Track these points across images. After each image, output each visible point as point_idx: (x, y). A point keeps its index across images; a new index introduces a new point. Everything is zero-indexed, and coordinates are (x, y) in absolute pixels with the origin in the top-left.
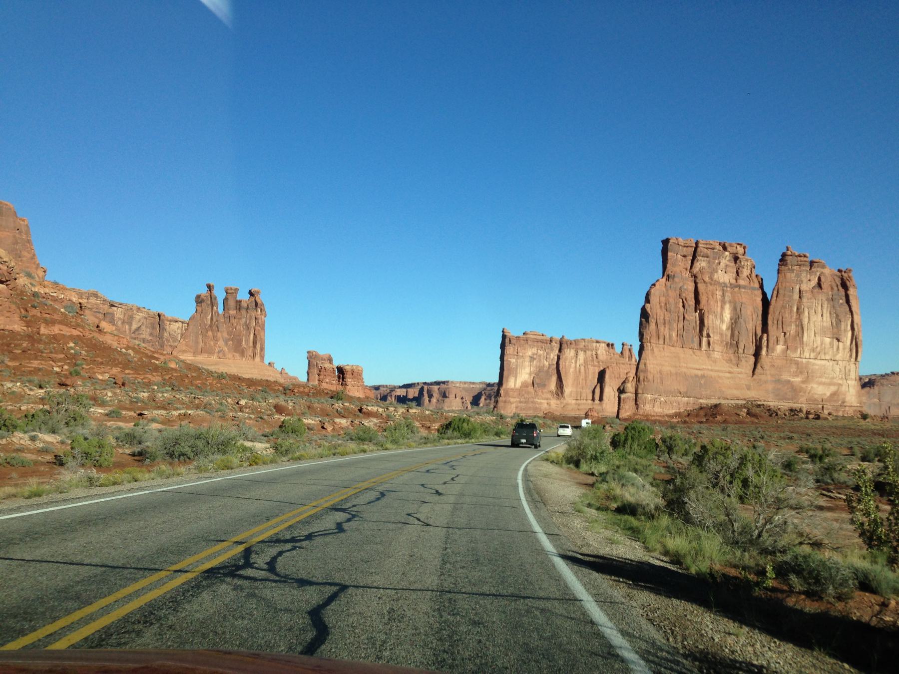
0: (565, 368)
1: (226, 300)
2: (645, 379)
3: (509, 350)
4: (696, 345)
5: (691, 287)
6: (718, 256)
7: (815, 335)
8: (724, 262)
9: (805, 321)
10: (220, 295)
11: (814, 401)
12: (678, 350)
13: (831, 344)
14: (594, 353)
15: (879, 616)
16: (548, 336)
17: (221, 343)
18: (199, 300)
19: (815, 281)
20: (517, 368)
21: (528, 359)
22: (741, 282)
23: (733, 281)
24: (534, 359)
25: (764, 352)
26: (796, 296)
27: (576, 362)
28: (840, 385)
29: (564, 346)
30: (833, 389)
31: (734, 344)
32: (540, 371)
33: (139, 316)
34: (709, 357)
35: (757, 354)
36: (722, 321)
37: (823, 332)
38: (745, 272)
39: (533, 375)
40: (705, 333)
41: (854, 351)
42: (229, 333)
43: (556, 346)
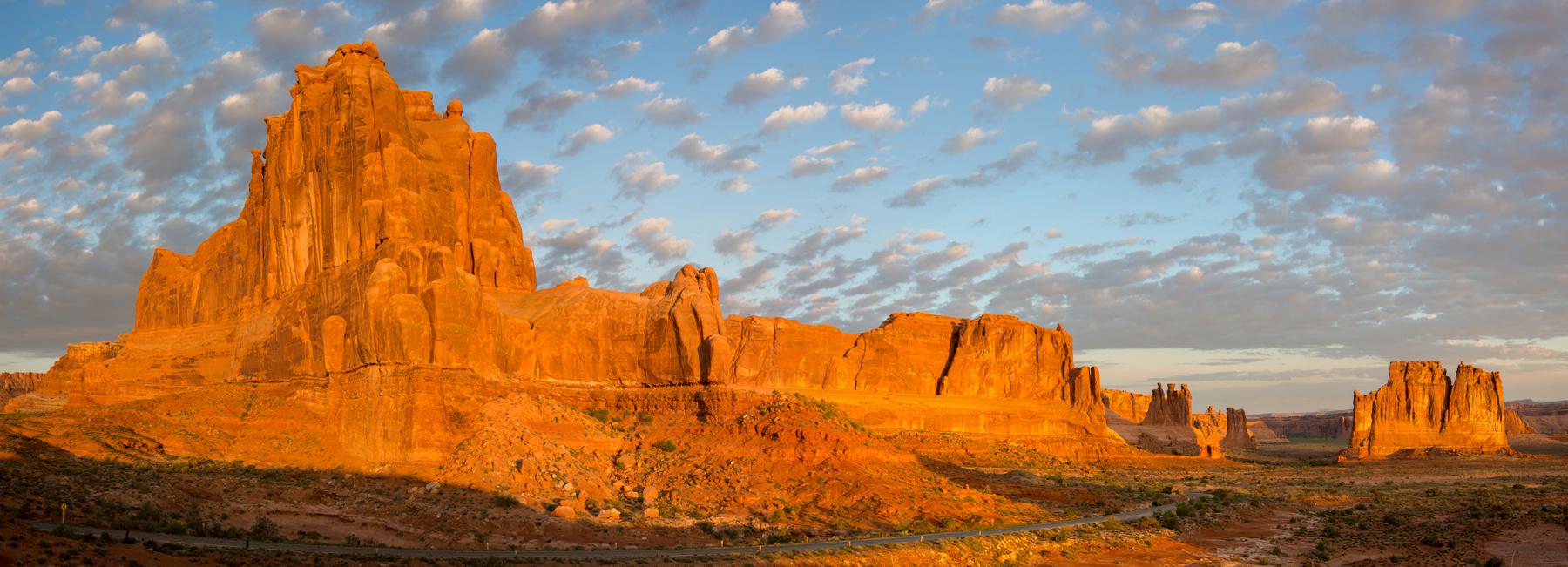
1: (1168, 392)
4: (1406, 418)
5: (1404, 388)
6: (1420, 369)
8: (1424, 372)
10: (1165, 389)
11: (1478, 444)
12: (1395, 422)
13: (1486, 413)
17: (1167, 416)
18: (1154, 392)
19: (1476, 380)
22: (1435, 382)
23: (1430, 382)
25: (1446, 420)
26: (1465, 388)
28: (1492, 434)
30: (1488, 436)
31: (1430, 416)
33: (1120, 397)
34: (1414, 423)
35: (1443, 420)
36: (1423, 403)
37: (1482, 406)
38: (1437, 377)
40: (1411, 412)
42: (1172, 411)
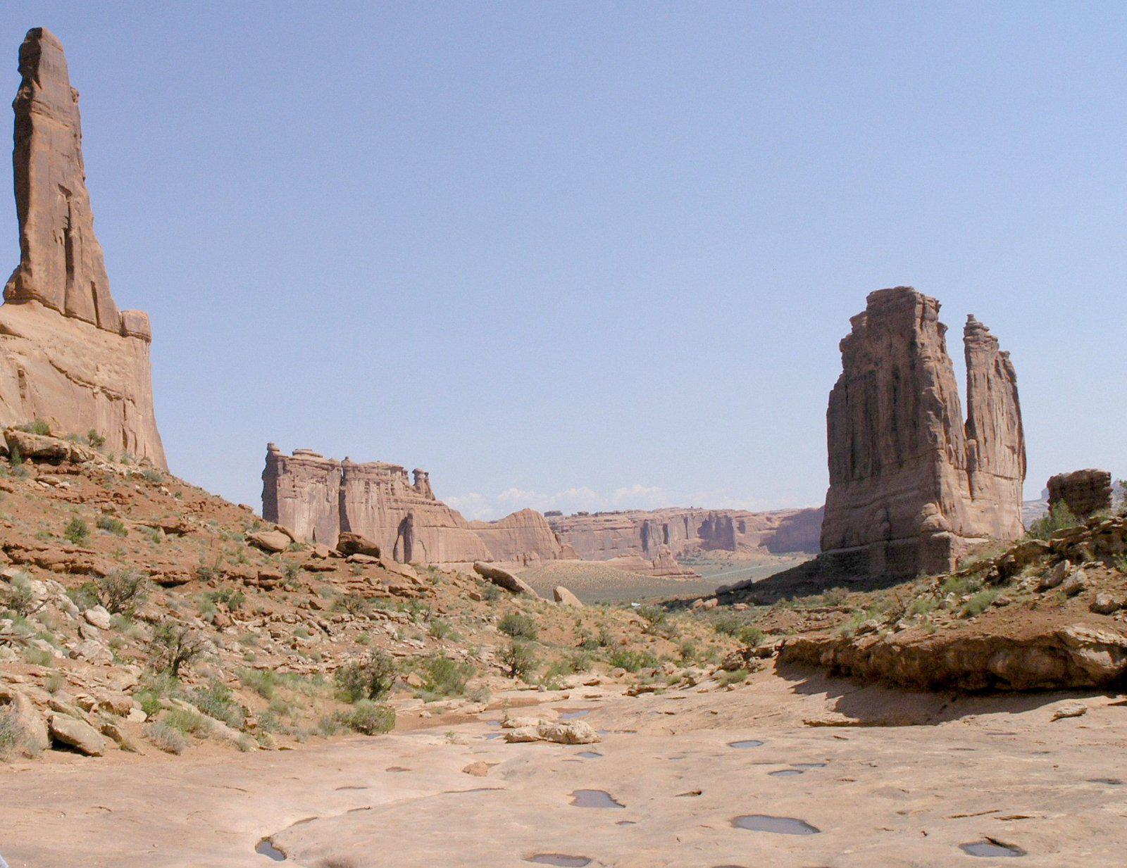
0: (354, 510)
2: (953, 508)
3: (284, 482)
7: (1001, 443)
9: (995, 424)
14: (390, 485)
15: (1078, 815)
16: (325, 459)
20: (294, 513)
21: (307, 497)
24: (314, 497)
27: (367, 501)
29: (350, 475)
32: (320, 518)
39: (313, 526)
41: (1022, 465)
43: (337, 475)
